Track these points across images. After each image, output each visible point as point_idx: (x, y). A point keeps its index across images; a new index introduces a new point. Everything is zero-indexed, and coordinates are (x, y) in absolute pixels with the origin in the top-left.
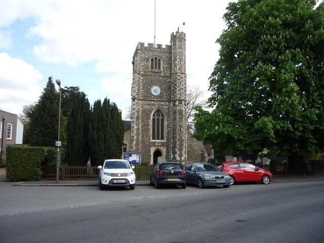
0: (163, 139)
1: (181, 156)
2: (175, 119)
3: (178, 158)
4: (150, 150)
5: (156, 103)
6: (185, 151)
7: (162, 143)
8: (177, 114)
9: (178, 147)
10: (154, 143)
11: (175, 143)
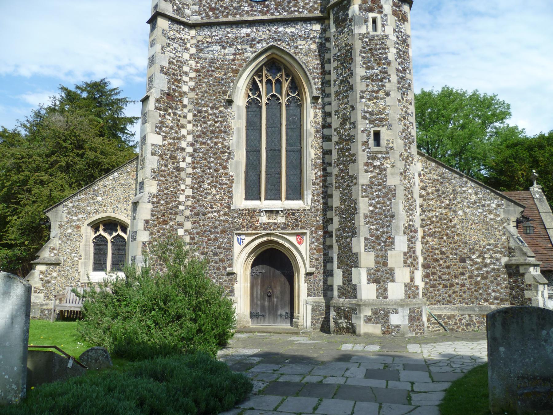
0: (300, 196)
1: (381, 276)
2: (348, 86)
3: (368, 292)
4: (229, 248)
5: (262, 32)
6: (410, 254)
7: (289, 213)
8: (358, 60)
9: (364, 231)
10: (253, 213)
11: (351, 210)
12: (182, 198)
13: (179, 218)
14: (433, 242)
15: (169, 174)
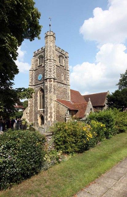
5: (40, 85)
10: (39, 111)
12: (33, 109)
13: (33, 112)
14: (57, 114)
15: (31, 107)
